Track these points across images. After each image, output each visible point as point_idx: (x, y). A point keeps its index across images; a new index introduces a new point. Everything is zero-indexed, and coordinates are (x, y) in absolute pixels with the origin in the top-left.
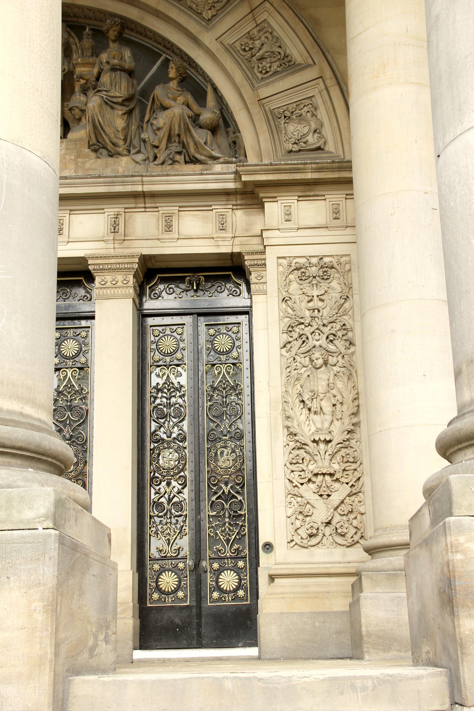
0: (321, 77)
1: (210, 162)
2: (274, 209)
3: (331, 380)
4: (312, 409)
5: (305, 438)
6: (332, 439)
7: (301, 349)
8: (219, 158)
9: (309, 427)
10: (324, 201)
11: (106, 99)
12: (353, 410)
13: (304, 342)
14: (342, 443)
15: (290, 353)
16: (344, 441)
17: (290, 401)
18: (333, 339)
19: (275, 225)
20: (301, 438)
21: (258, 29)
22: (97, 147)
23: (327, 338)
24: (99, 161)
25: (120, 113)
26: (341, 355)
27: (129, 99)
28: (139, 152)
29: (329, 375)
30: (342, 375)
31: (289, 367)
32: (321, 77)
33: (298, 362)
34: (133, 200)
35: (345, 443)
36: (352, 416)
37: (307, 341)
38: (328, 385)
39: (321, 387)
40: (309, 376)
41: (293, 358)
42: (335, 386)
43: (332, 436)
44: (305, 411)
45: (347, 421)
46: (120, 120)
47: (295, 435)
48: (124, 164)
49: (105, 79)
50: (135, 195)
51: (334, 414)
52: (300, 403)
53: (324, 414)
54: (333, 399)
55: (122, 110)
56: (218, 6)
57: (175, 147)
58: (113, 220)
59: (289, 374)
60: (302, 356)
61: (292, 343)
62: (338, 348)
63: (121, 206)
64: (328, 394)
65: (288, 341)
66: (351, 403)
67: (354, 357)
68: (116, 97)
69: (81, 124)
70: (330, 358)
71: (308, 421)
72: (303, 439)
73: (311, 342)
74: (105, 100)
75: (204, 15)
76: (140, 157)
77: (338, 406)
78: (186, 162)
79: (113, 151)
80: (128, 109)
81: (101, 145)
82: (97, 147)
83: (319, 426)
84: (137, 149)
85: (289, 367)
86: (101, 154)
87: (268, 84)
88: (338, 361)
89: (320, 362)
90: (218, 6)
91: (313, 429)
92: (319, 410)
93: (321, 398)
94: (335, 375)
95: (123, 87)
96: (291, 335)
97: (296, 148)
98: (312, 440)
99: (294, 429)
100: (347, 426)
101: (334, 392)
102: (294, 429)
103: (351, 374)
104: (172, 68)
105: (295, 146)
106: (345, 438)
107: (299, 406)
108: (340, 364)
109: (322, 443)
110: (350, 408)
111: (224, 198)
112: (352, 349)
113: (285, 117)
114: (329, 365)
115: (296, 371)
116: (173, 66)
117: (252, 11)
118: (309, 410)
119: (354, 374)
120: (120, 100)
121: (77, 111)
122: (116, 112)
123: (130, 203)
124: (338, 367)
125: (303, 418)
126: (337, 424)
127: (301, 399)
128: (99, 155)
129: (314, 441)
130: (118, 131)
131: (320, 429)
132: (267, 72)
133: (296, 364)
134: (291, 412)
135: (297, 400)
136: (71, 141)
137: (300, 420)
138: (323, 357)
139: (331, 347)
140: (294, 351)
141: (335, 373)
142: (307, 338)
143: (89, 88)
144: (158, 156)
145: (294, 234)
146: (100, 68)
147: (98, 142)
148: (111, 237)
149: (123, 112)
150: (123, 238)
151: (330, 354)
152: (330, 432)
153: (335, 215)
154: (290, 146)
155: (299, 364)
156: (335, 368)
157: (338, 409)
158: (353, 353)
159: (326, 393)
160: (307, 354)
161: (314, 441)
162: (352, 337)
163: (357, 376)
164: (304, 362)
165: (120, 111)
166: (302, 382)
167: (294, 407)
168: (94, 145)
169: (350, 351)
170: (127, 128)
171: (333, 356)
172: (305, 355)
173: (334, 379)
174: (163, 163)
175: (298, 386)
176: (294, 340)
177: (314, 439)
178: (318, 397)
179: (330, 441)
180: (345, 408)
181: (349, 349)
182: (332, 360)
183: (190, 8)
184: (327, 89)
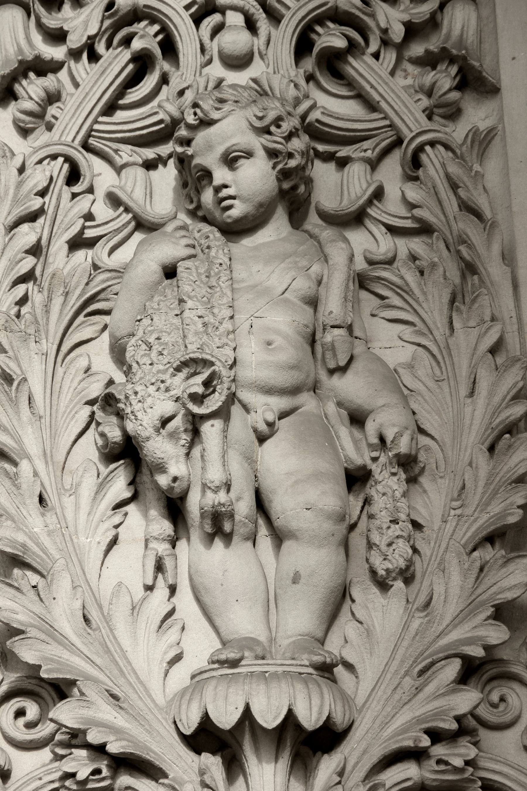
3: (333, 305)
4: (195, 503)
5: (136, 717)
6: (340, 720)
7: (120, 115)
9: (172, 635)
12: (495, 508)
13: (142, 63)
14: (416, 755)
15: (41, 137)
16: (436, 736)
17: (32, 446)
18: (340, 43)
20: (106, 712)
23: (303, 46)
26: (396, 156)
29: (316, 268)
30: (411, 278)
31: (32, 217)
33: (100, 192)
35: (439, 751)
36: (488, 553)
37: (163, 65)
38: (312, 341)
39: (261, 344)
40: (170, 272)
41: (59, 169)
42: (359, 349)
43: (346, 699)
44: (145, 524)
45: (450, 584)
47: (61, 690)
51: (357, 541)
52: (104, 471)
53: (279, 537)
54: (345, 434)
59: (29, 262)
60: (126, 154)
61: (63, 75)
62: (371, 106)
64: (307, 402)
65: (29, 56)
66: (482, 460)
67: (492, 169)
70: (323, 174)
71: (161, 592)
72: (119, 720)
73: (192, 71)
77: (387, 483)
83: (244, 621)
85: (32, 217)
88: (379, 194)
89: (254, 179)
91: (200, 646)
92: (244, 507)
93: (258, 420)
94: (362, 282)
96: (52, 21)
98: (190, 725)
99: (54, 650)
100: (458, 620)
101: (353, 386)
102: (54, 650)
103: (469, 269)
106: (439, 714)
107: (102, 487)
108: (392, 209)
109: (268, 749)
110: (474, 498)
112: (477, 115)
114: (313, 221)
115: (82, 256)
118: (174, 508)
119: (495, 270)
124: (379, 231)
125: (129, 566)
126: (380, 613)
127: (115, 434)
129: (205, 738)
131: (250, 643)
133: (83, 204)
134: (36, 521)
135: (89, 448)
137: (106, 588)
138: (275, 141)
139: (335, 107)
140: (70, 121)
141: (360, 265)
142: (169, 48)
151: (321, 148)
152: (325, 670)
155: (102, 211)
156: (359, 240)
157: (380, 504)
158: (483, 142)
159: (294, 391)
160: (164, 150)
161: (205, 738)
162: (471, 37)
163: (515, 286)
164: (139, 194)
166: (121, 319)
167: (61, 490)
169: (458, 132)
171: (343, 163)
172: (150, 153)
173: (351, 302)
175: (99, 356)
176: (75, 54)
177: (206, 724)
178: (236, 410)
179: (328, 738)
180: (432, 501)
181: (453, 113)
182: (333, 186)
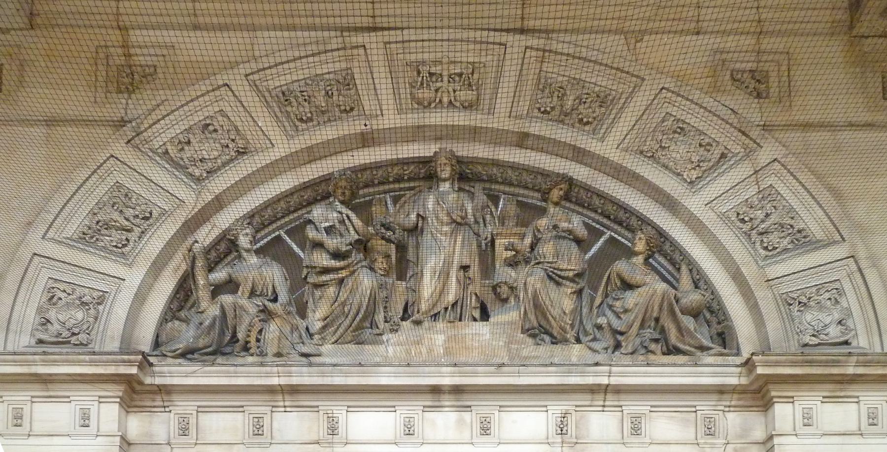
0: (852, 257)
1: (699, 353)
2: (783, 413)
8: (711, 348)
10: (855, 405)
19: (788, 428)
21: (760, 196)
24: (542, 349)
25: (569, 291)
27: (579, 275)
28: (595, 339)
32: (852, 257)
34: (589, 396)
48: (576, 351)
49: (547, 249)
50: (593, 390)
56: (705, 165)
57: (648, 333)
58: (559, 419)
63: (571, 403)
68: (566, 270)
75: (685, 177)
76: (597, 346)
78: (664, 354)
79: (558, 337)
80: (579, 286)
84: (591, 337)
86: (543, 340)
87: (776, 262)
90: (705, 165)
97: (815, 341)
104: (640, 239)
105: (813, 338)
111: (715, 397)
113: (800, 303)
116: (642, 236)
117: (756, 172)
120: (571, 274)
122: (562, 289)
123: (584, 399)
128: (540, 342)
130: (564, 313)
132: (775, 248)
144: (623, 344)
145: (817, 441)
146: (535, 236)
147: (540, 326)
148: (559, 439)
150: (575, 441)
153: (871, 421)
154: (807, 339)
165: (569, 288)
168: (533, 328)
170: (577, 311)
174: (632, 353)
183: (666, 167)
184: (860, 270)
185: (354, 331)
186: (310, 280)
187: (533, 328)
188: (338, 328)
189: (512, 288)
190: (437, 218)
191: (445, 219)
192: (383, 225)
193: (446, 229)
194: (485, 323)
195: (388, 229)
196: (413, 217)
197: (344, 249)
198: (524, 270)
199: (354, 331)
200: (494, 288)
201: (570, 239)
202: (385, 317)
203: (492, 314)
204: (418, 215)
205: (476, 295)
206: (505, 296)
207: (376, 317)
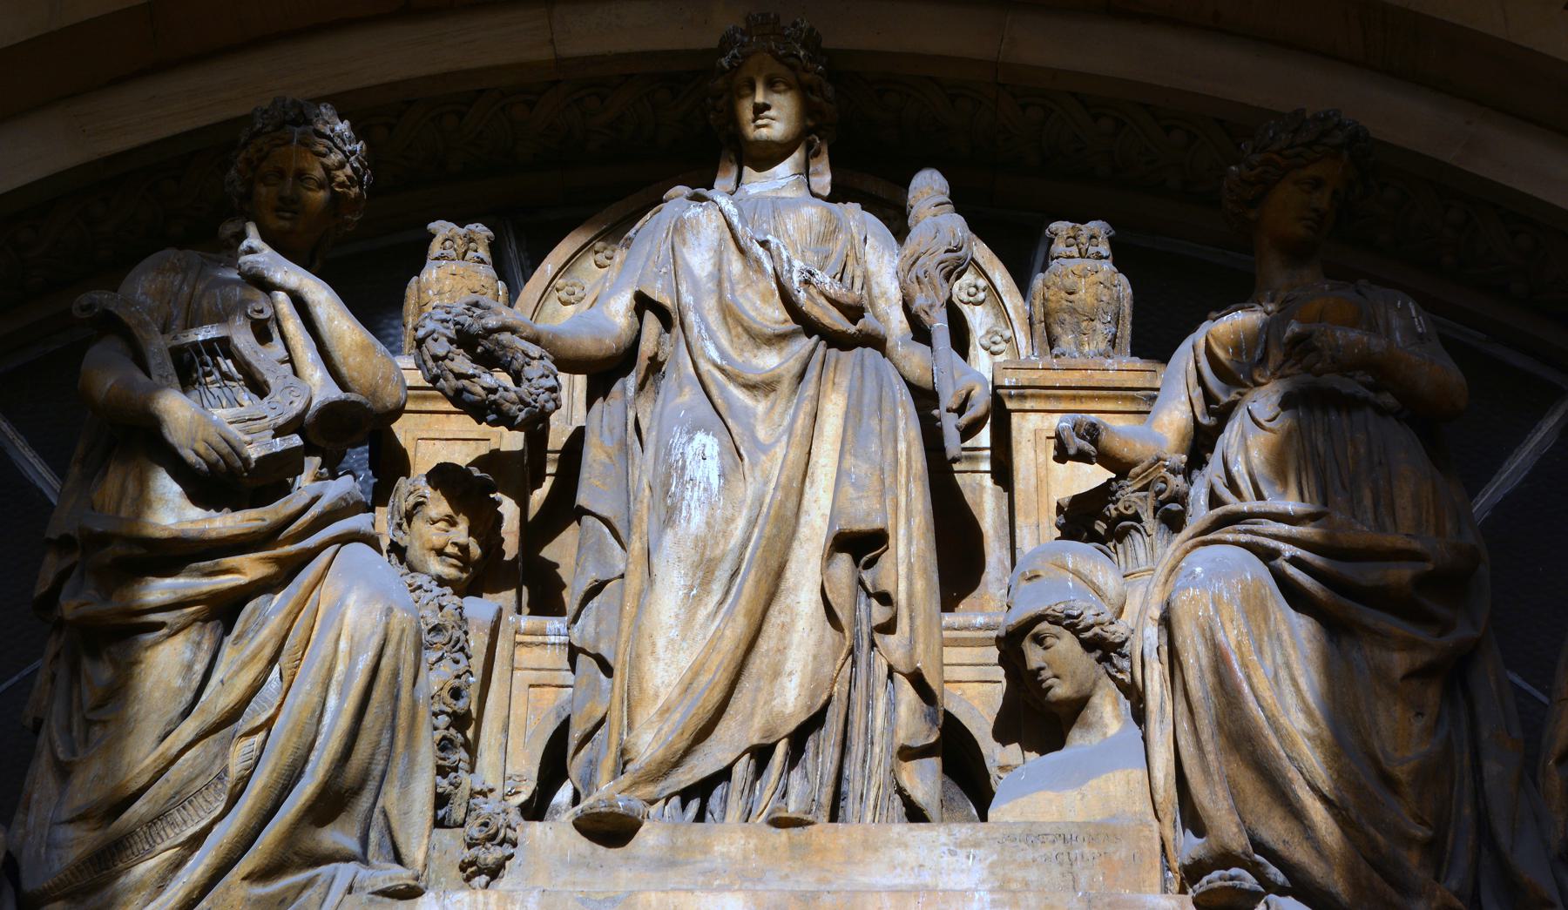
11: (1294, 561)
22: (1249, 882)
25: (1399, 662)
27: (1448, 582)
46: (1398, 710)
55: (1410, 645)
69: (1078, 740)
74: (1291, 570)
80: (1449, 640)
81: (1275, 873)
82: (1249, 882)
95: (1404, 500)
120: (1402, 573)
121: (1066, 645)
130: (1389, 781)
136: (1033, 835)
143: (1137, 517)
147: (1259, 846)
149: (1422, 658)
185: (263, 874)
186: (69, 607)
187: (1226, 859)
188: (177, 865)
189: (1103, 648)
190: (729, 313)
191: (773, 316)
192: (465, 340)
193: (769, 361)
194: (964, 831)
195: (490, 361)
196: (619, 310)
197: (254, 453)
198: (1151, 550)
199: (263, 874)
200: (1011, 645)
201: (1381, 411)
202: (441, 800)
203: (1000, 784)
204: (643, 303)
205: (917, 680)
206: (1061, 690)
207: (391, 797)
